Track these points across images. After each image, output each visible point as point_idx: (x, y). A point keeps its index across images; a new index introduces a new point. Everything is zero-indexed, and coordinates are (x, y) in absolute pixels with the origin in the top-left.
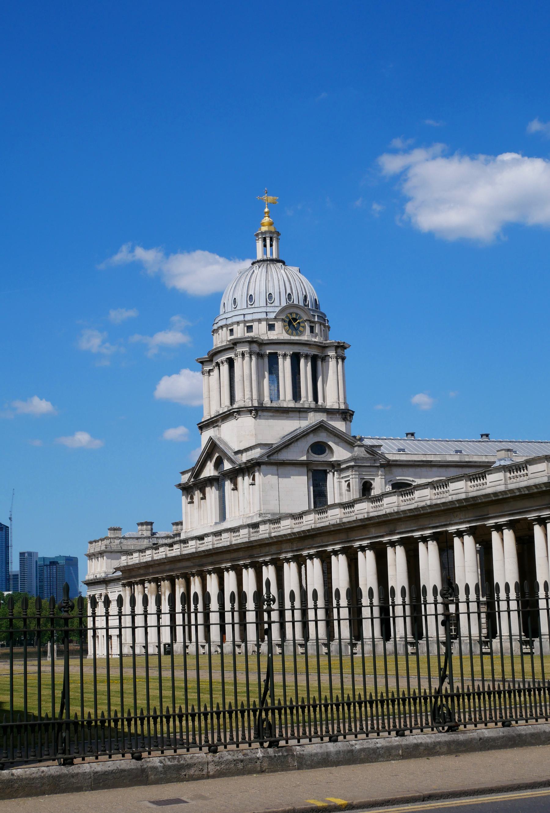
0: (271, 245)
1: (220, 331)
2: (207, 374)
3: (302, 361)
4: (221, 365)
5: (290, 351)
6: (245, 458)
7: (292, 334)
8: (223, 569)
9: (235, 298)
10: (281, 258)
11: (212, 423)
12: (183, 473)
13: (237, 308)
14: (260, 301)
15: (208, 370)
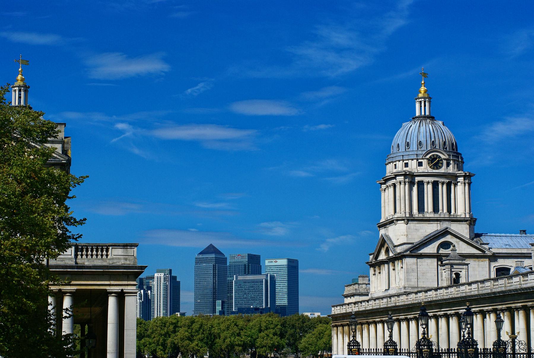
0: (425, 106)
1: (389, 164)
2: (384, 191)
3: (440, 186)
4: (389, 187)
5: (431, 179)
6: (399, 250)
7: (434, 169)
8: (376, 322)
9: (398, 144)
10: (432, 115)
11: (384, 225)
12: (370, 255)
13: (400, 151)
14: (414, 146)
15: (384, 189)
